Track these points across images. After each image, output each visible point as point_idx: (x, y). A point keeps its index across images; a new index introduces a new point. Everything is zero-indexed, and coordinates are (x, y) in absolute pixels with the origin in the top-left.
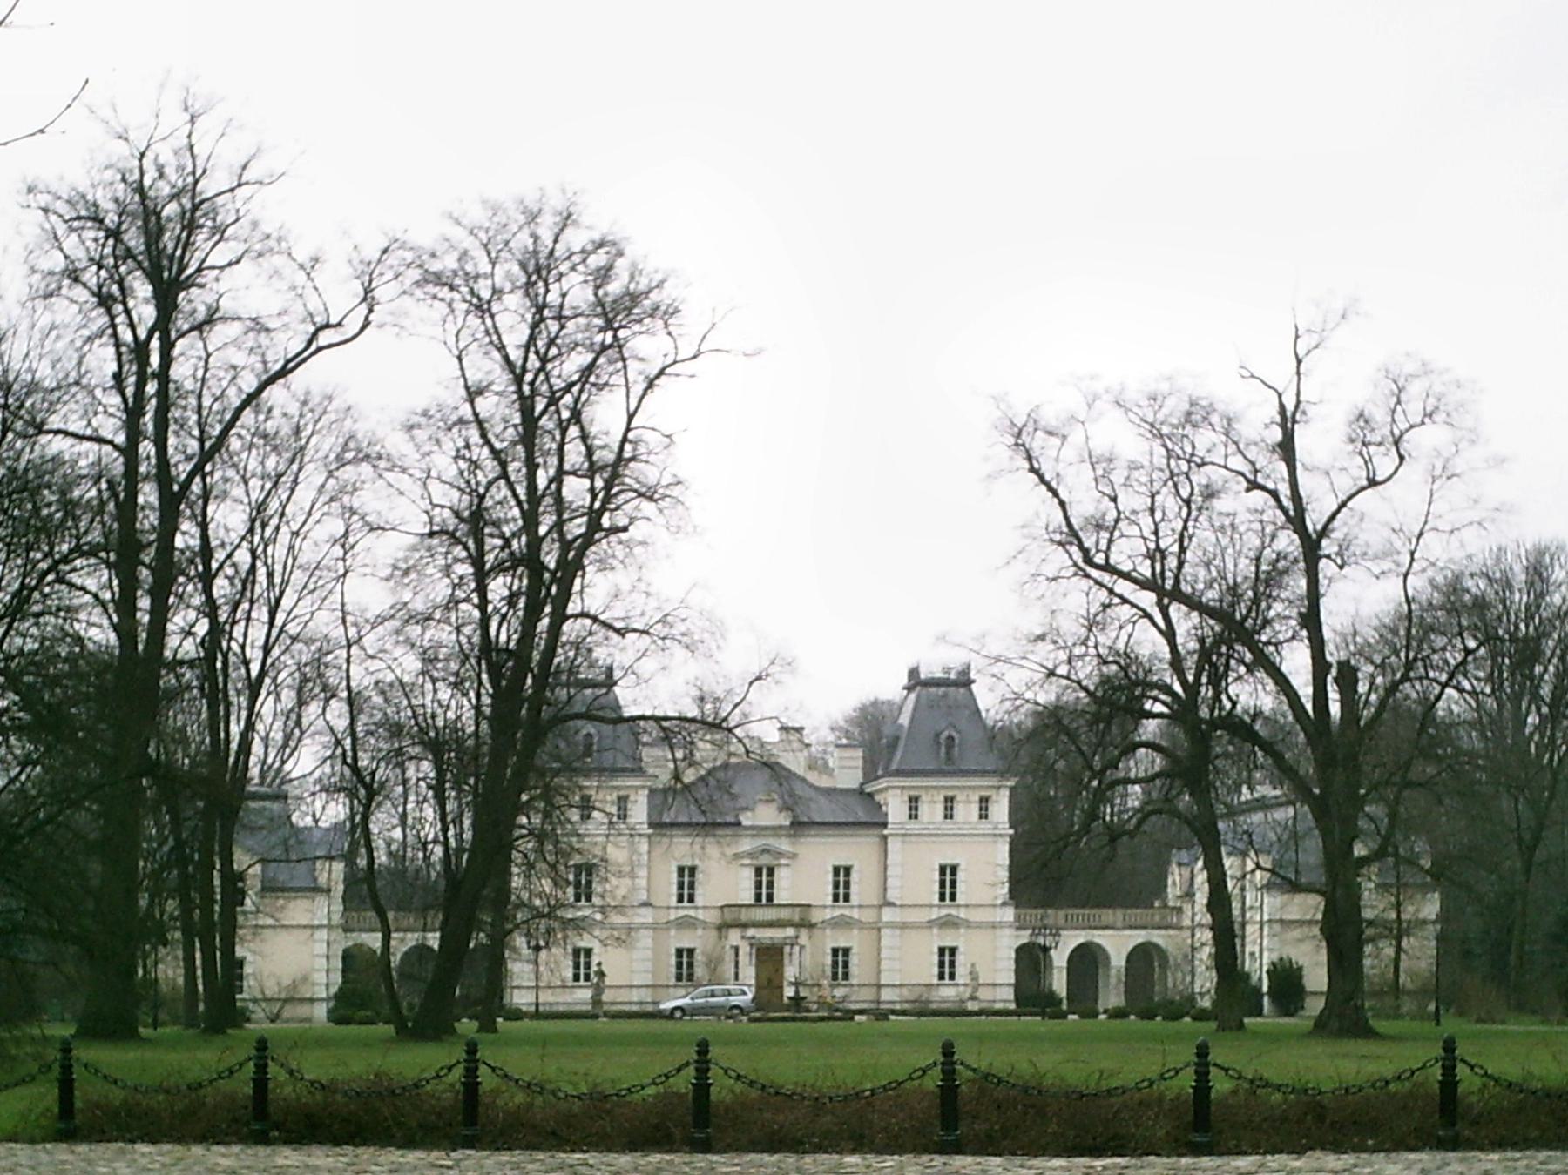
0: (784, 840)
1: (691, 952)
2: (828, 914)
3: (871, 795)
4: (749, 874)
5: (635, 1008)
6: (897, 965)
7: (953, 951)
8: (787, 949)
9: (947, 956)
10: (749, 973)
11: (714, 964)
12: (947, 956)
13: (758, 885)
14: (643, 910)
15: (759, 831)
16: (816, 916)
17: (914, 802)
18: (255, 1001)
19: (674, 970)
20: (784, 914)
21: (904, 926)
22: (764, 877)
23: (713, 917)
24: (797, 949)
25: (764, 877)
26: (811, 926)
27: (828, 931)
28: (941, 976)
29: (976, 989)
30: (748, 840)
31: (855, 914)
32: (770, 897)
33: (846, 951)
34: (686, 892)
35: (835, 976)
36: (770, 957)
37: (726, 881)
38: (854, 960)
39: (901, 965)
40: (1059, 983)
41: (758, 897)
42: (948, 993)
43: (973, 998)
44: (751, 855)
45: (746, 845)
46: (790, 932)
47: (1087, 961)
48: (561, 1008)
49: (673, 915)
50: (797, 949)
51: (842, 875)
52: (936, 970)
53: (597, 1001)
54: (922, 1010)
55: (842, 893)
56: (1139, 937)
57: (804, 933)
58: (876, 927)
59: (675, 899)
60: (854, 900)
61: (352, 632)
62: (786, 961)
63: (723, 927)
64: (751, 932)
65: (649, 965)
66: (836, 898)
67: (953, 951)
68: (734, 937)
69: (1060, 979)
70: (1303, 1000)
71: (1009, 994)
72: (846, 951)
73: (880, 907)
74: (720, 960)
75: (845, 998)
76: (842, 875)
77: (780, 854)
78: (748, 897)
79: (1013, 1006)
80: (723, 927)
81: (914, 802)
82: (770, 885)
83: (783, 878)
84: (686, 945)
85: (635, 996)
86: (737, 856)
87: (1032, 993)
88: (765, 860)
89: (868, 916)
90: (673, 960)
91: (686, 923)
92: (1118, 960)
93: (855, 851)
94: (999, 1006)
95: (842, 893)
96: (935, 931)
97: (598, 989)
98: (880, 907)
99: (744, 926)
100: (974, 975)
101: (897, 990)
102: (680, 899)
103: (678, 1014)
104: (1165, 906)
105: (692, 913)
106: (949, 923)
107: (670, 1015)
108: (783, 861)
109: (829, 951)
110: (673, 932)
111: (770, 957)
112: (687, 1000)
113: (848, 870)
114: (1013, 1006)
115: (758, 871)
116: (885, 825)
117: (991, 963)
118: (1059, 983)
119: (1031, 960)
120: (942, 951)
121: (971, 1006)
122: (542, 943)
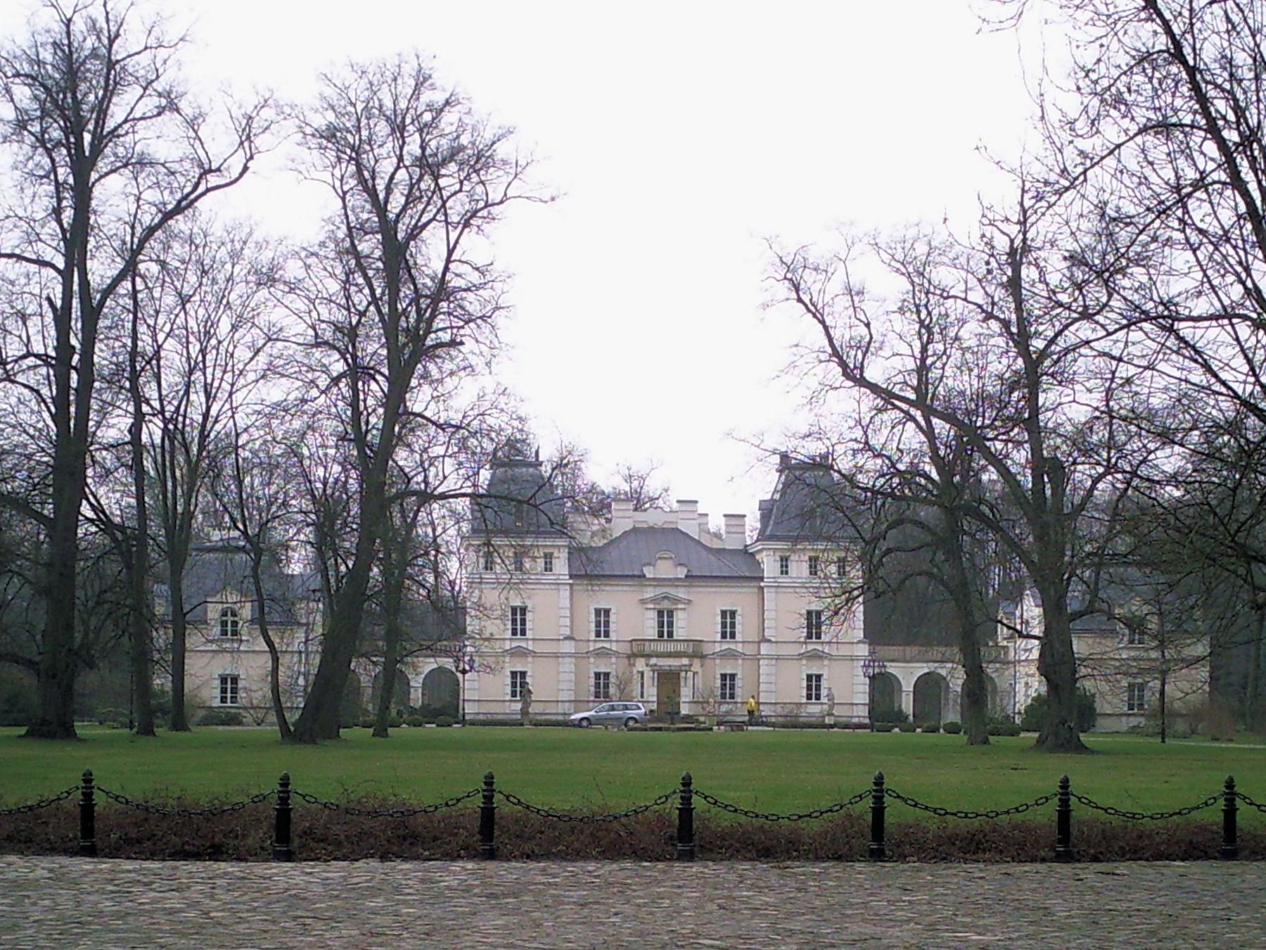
0: (683, 589)
1: (607, 675)
2: (718, 648)
3: (752, 554)
4: (654, 615)
5: (560, 718)
6: (773, 688)
7: (819, 677)
8: (683, 674)
9: (814, 682)
10: (652, 693)
11: (623, 686)
12: (814, 682)
13: (661, 625)
14: (567, 642)
15: (659, 582)
16: (708, 649)
17: (784, 561)
18: (245, 708)
19: (593, 689)
20: (681, 647)
21: (778, 658)
22: (665, 620)
23: (625, 649)
24: (690, 674)
25: (665, 620)
26: (703, 657)
27: (718, 661)
28: (809, 697)
29: (831, 707)
30: (651, 589)
31: (739, 648)
32: (670, 634)
33: (733, 676)
34: (665, 629)
35: (723, 696)
36: (669, 681)
37: (633, 618)
38: (738, 683)
39: (778, 686)
40: (907, 704)
41: (661, 634)
42: (814, 709)
43: (830, 714)
44: (653, 600)
45: (650, 593)
46: (685, 661)
47: (929, 687)
48: (499, 717)
49: (592, 647)
50: (690, 674)
51: (728, 617)
52: (804, 692)
53: (524, 712)
54: (792, 723)
55: (728, 632)
56: (922, 669)
57: (697, 662)
58: (757, 658)
59: (593, 634)
60: (739, 637)
61: (938, 292)
62: (682, 684)
63: (632, 656)
64: (653, 661)
65: (572, 686)
66: (724, 636)
67: (819, 677)
68: (640, 664)
69: (907, 703)
70: (1095, 720)
71: (863, 711)
72: (733, 676)
73: (759, 642)
74: (629, 681)
75: (728, 713)
76: (728, 617)
77: (677, 600)
78: (652, 633)
79: (867, 721)
80: (632, 656)
81: (784, 561)
82: (671, 624)
83: (680, 620)
84: (603, 670)
85: (561, 708)
86: (643, 601)
87: (883, 712)
88: (666, 605)
89: (750, 650)
90: (592, 681)
91: (602, 654)
92: (908, 685)
93: (739, 599)
94: (855, 720)
95: (728, 632)
96: (804, 662)
97: (526, 704)
98: (759, 642)
99: (649, 656)
100: (830, 697)
101: (773, 708)
102: (598, 635)
103: (585, 723)
104: (997, 645)
105: (607, 645)
106: (816, 656)
107: (579, 724)
108: (680, 606)
109: (719, 676)
110: (592, 660)
111: (669, 681)
112: (592, 713)
113: (733, 613)
114: (867, 721)
115: (660, 613)
116: (762, 579)
117: (849, 691)
118: (907, 704)
119: (882, 685)
120: (809, 677)
121: (827, 720)
122: (467, 668)
